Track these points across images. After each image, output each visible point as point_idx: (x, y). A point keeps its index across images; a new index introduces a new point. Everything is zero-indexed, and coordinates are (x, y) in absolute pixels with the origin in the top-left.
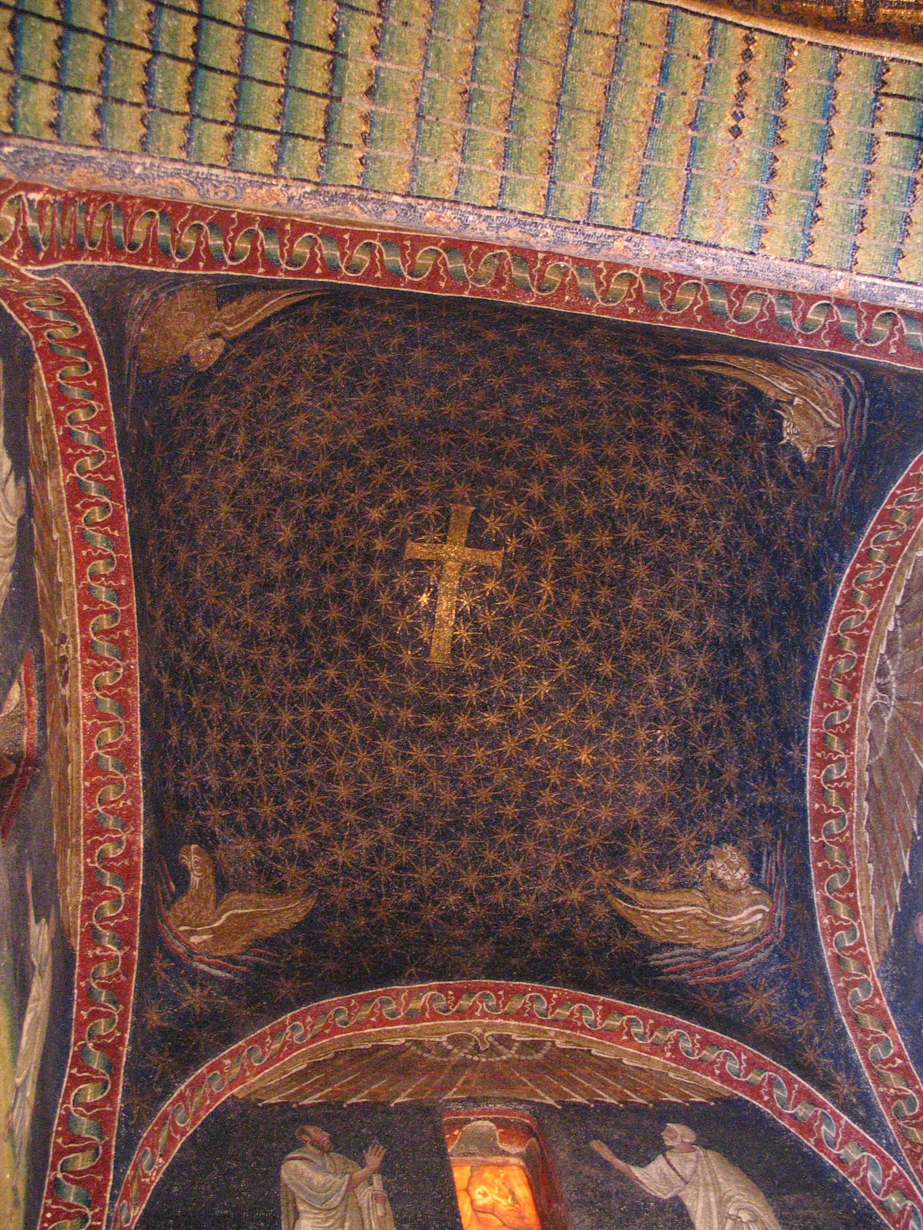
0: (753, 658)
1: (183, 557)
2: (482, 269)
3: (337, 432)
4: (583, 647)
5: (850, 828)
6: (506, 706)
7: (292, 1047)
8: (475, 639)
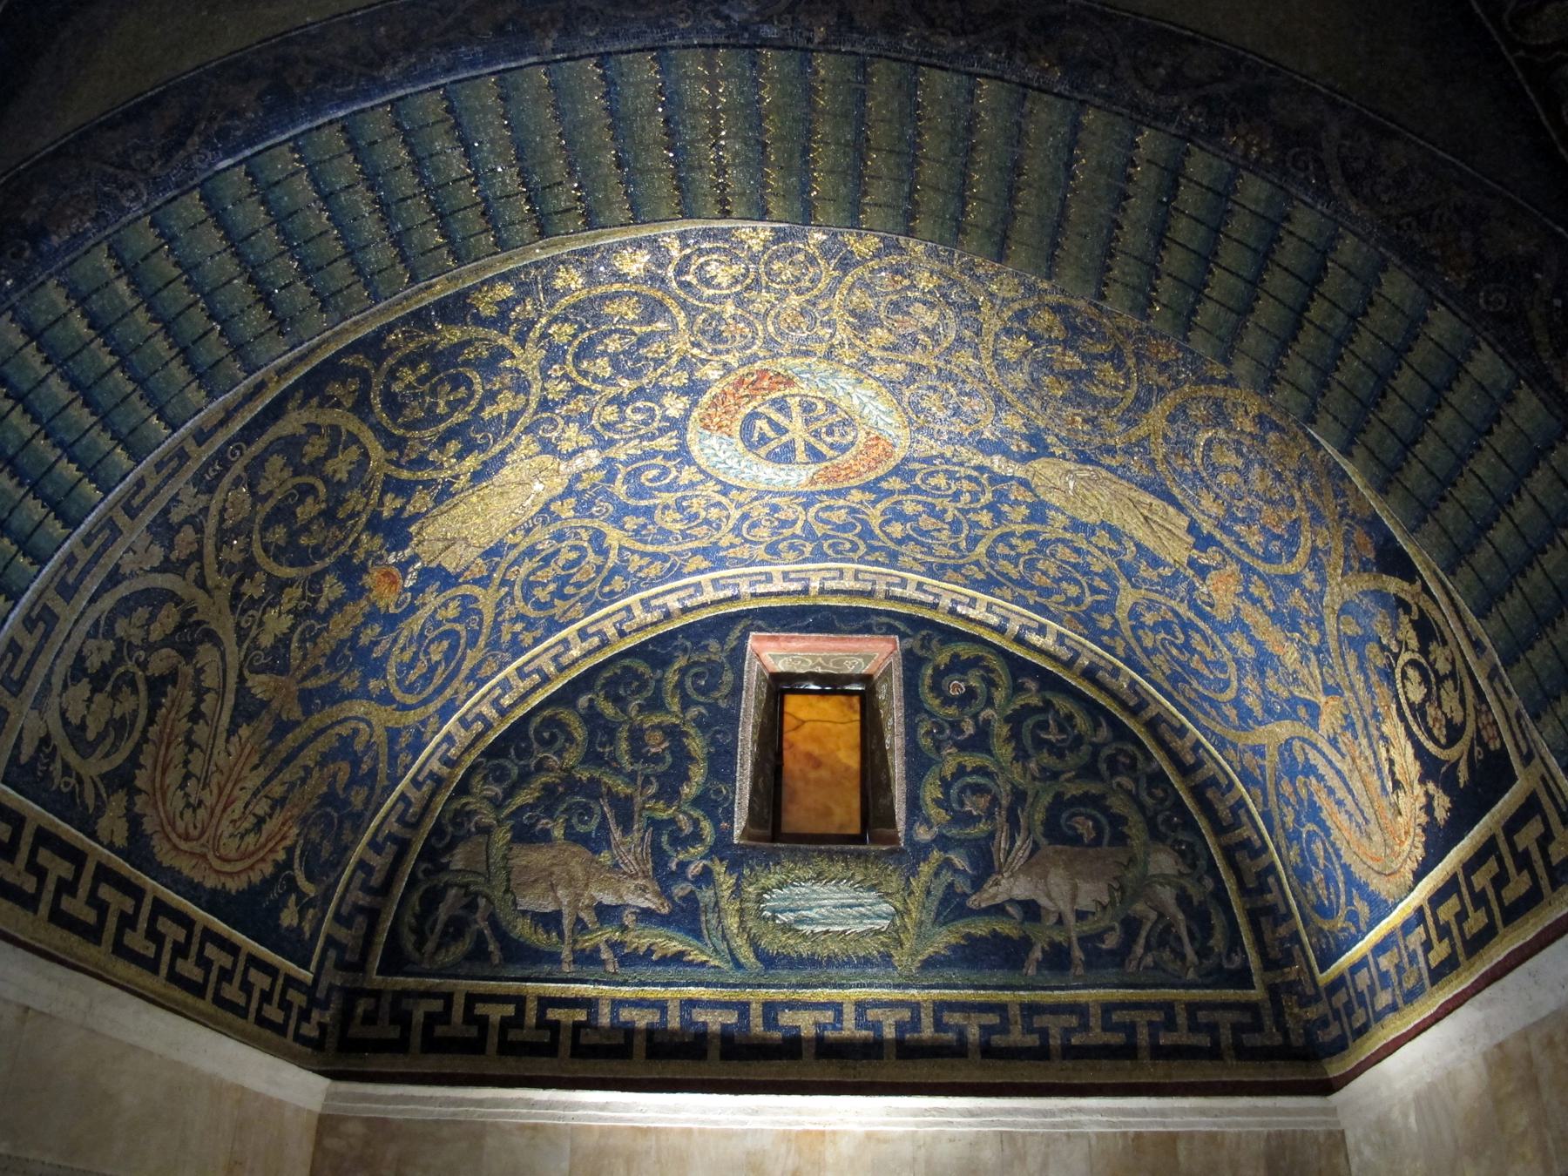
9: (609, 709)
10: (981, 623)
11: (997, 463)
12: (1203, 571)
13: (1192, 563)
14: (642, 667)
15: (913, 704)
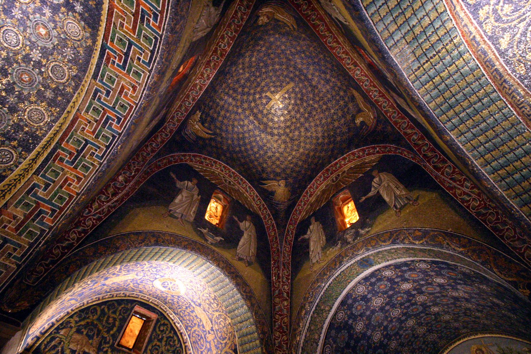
0: (229, 63)
1: (312, 154)
2: (237, 179)
3: (277, 141)
4: (264, 70)
5: (226, 30)
6: (287, 69)
7: (380, 92)
8: (283, 82)
9: (106, 310)
10: (171, 318)
11: (192, 304)
12: (209, 333)
13: (209, 331)
14: (116, 305)
15: (154, 329)
